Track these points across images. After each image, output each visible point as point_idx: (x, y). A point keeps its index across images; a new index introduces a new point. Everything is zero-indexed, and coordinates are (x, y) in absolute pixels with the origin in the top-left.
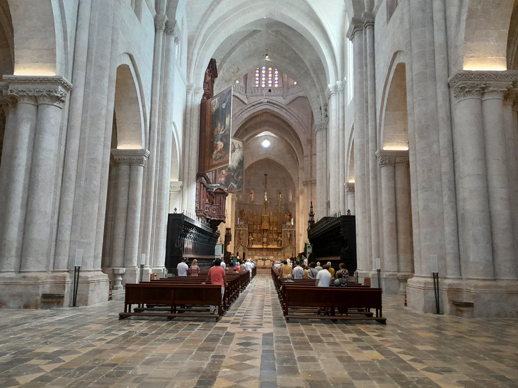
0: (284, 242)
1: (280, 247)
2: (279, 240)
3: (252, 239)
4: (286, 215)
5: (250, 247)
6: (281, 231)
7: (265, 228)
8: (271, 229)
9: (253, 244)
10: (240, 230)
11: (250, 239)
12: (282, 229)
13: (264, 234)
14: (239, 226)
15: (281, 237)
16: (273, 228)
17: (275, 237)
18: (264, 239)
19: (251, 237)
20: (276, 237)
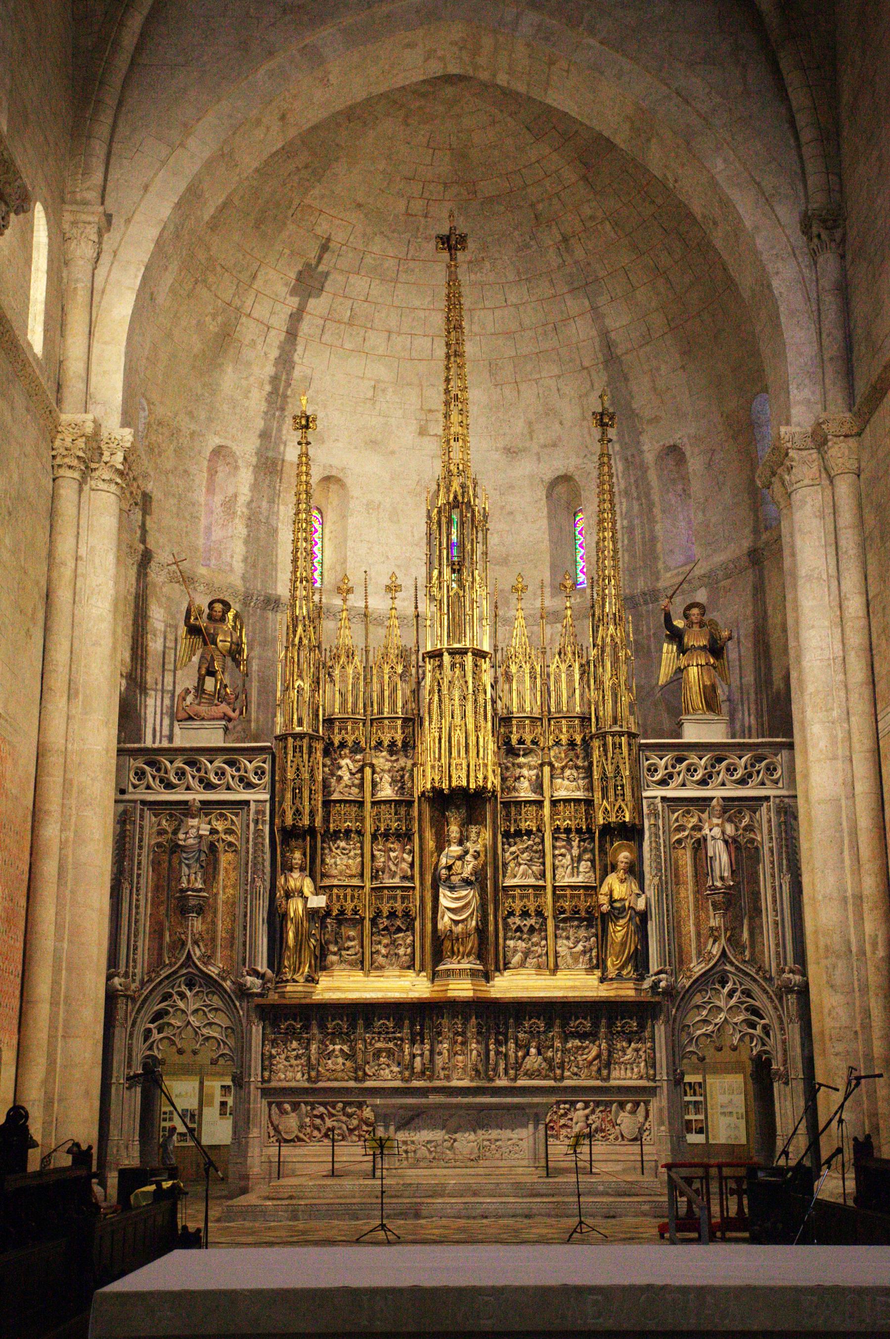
0: (674, 928)
1: (627, 991)
2: (616, 912)
3: (318, 901)
4: (669, 649)
5: (295, 989)
6: (638, 809)
7: (459, 779)
8: (525, 792)
9: (321, 964)
10: (184, 809)
11: (296, 907)
12: (637, 785)
13: (441, 844)
14: (171, 767)
15: (635, 871)
16: (538, 787)
17: (566, 879)
18: (446, 900)
19: (296, 880)
20: (584, 876)
